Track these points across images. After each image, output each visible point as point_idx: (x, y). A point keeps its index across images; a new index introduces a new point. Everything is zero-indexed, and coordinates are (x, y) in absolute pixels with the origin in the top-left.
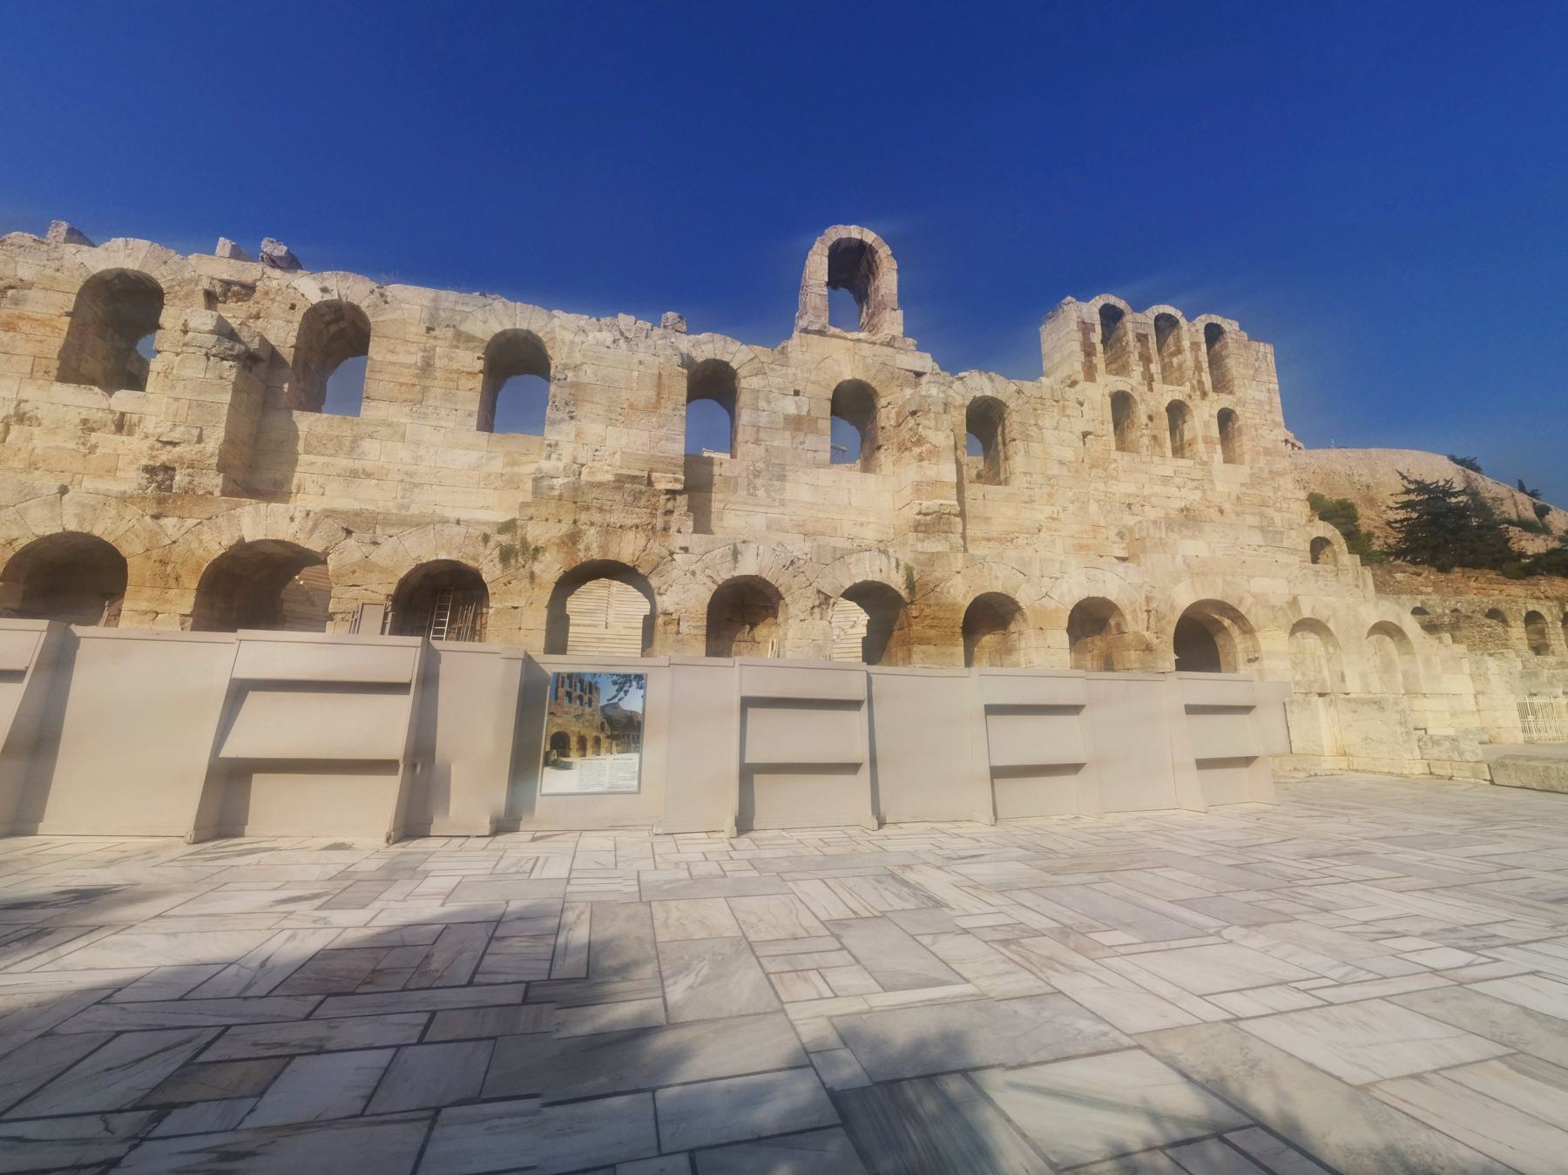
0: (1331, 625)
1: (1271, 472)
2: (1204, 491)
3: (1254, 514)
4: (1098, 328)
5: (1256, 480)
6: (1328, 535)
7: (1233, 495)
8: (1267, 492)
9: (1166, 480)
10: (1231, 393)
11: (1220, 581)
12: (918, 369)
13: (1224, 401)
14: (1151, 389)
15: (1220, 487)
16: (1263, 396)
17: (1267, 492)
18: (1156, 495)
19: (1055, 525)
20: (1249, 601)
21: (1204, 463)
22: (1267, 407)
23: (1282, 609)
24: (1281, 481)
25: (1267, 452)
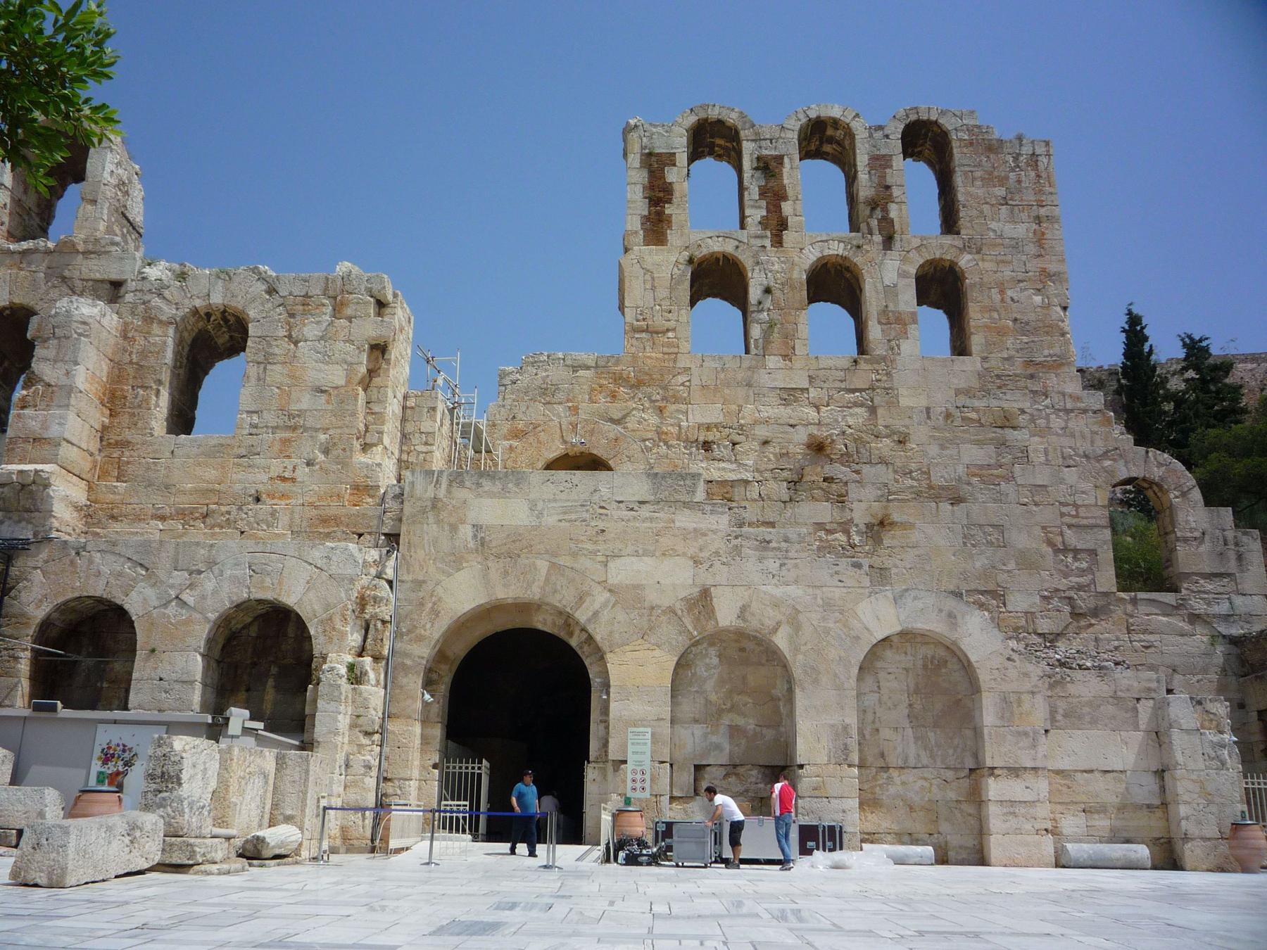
0: (781, 640)
1: (1029, 363)
2: (873, 410)
3: (979, 443)
4: (682, 158)
5: (992, 382)
6: (1156, 473)
7: (938, 410)
8: (1014, 401)
9: (789, 396)
10: (958, 233)
11: (543, 565)
12: (114, 276)
13: (942, 247)
14: (778, 241)
15: (906, 400)
16: (1021, 230)
17: (1014, 401)
18: (766, 422)
19: (282, 486)
20: (601, 597)
21: (884, 359)
22: (1032, 249)
23: (671, 610)
24: (1052, 381)
25: (1022, 326)
